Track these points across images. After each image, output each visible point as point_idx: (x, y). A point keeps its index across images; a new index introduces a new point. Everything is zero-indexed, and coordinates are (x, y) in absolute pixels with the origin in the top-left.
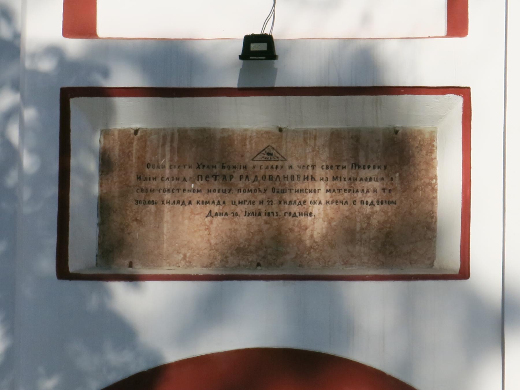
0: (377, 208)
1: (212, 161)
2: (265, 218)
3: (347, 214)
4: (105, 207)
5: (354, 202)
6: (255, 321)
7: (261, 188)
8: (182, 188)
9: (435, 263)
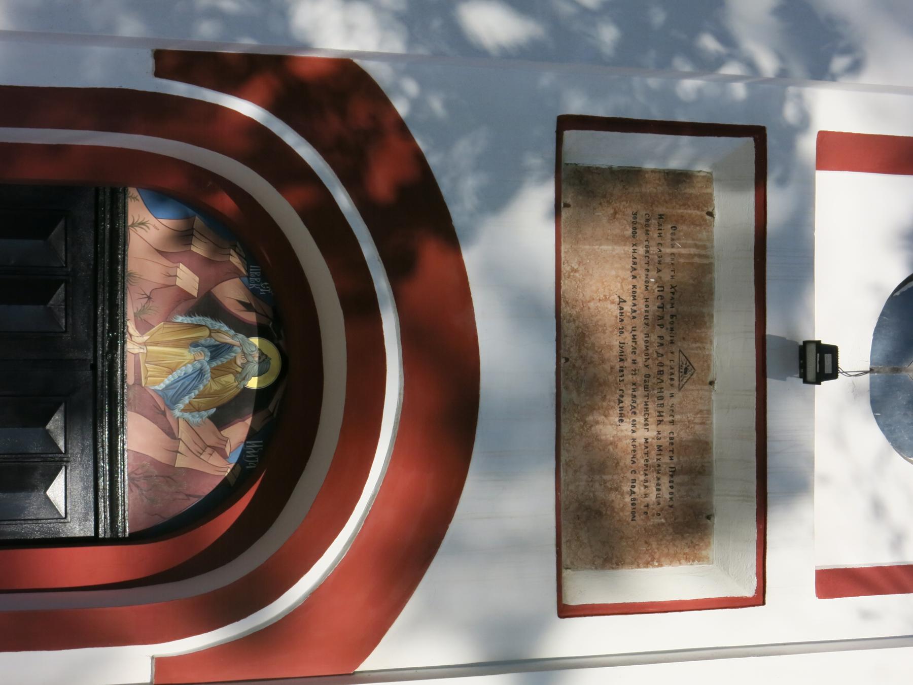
0: (628, 499)
2: (618, 367)
3: (622, 464)
4: (629, 176)
5: (634, 472)
6: (509, 357)
7: (650, 362)
8: (651, 267)
9: (569, 571)
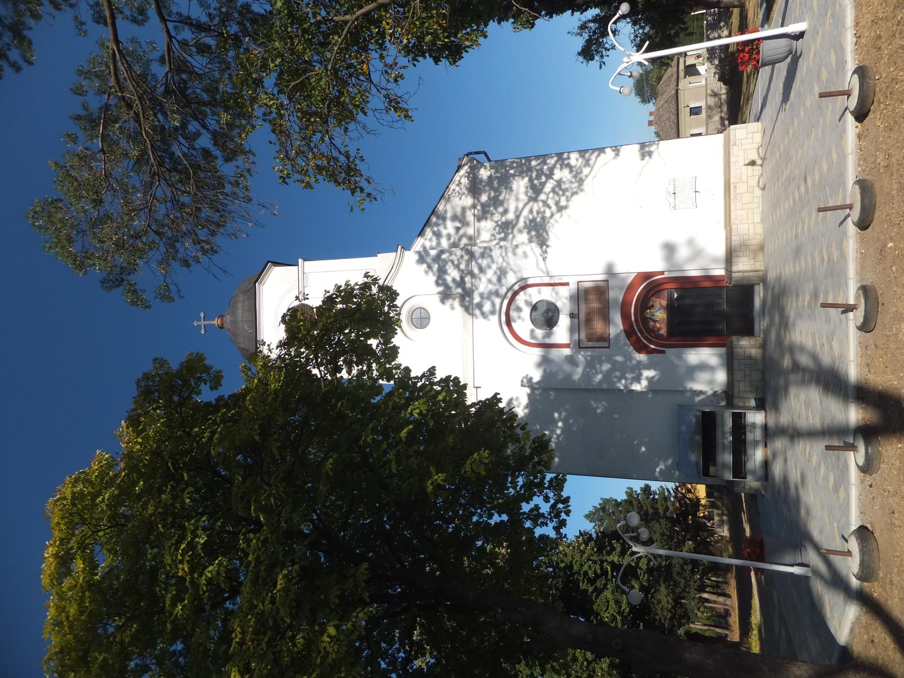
1: (589, 321)
